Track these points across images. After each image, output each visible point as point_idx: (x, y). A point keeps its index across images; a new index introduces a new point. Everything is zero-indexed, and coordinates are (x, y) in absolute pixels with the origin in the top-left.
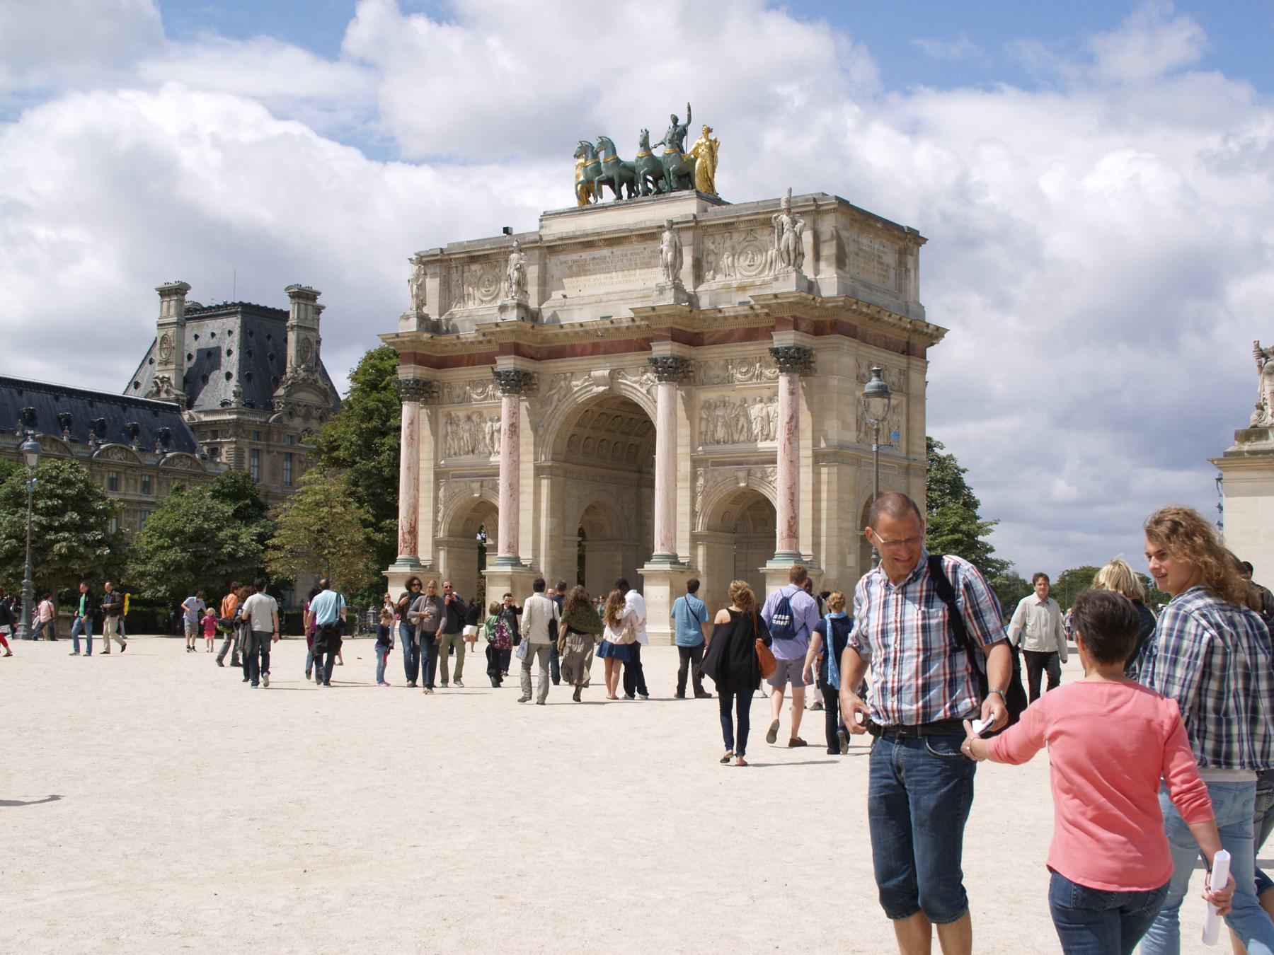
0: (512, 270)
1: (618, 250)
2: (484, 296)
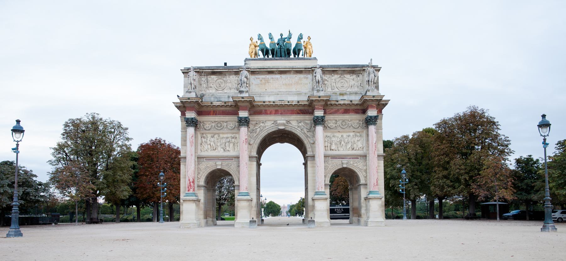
0: (244, 77)
1: (283, 76)
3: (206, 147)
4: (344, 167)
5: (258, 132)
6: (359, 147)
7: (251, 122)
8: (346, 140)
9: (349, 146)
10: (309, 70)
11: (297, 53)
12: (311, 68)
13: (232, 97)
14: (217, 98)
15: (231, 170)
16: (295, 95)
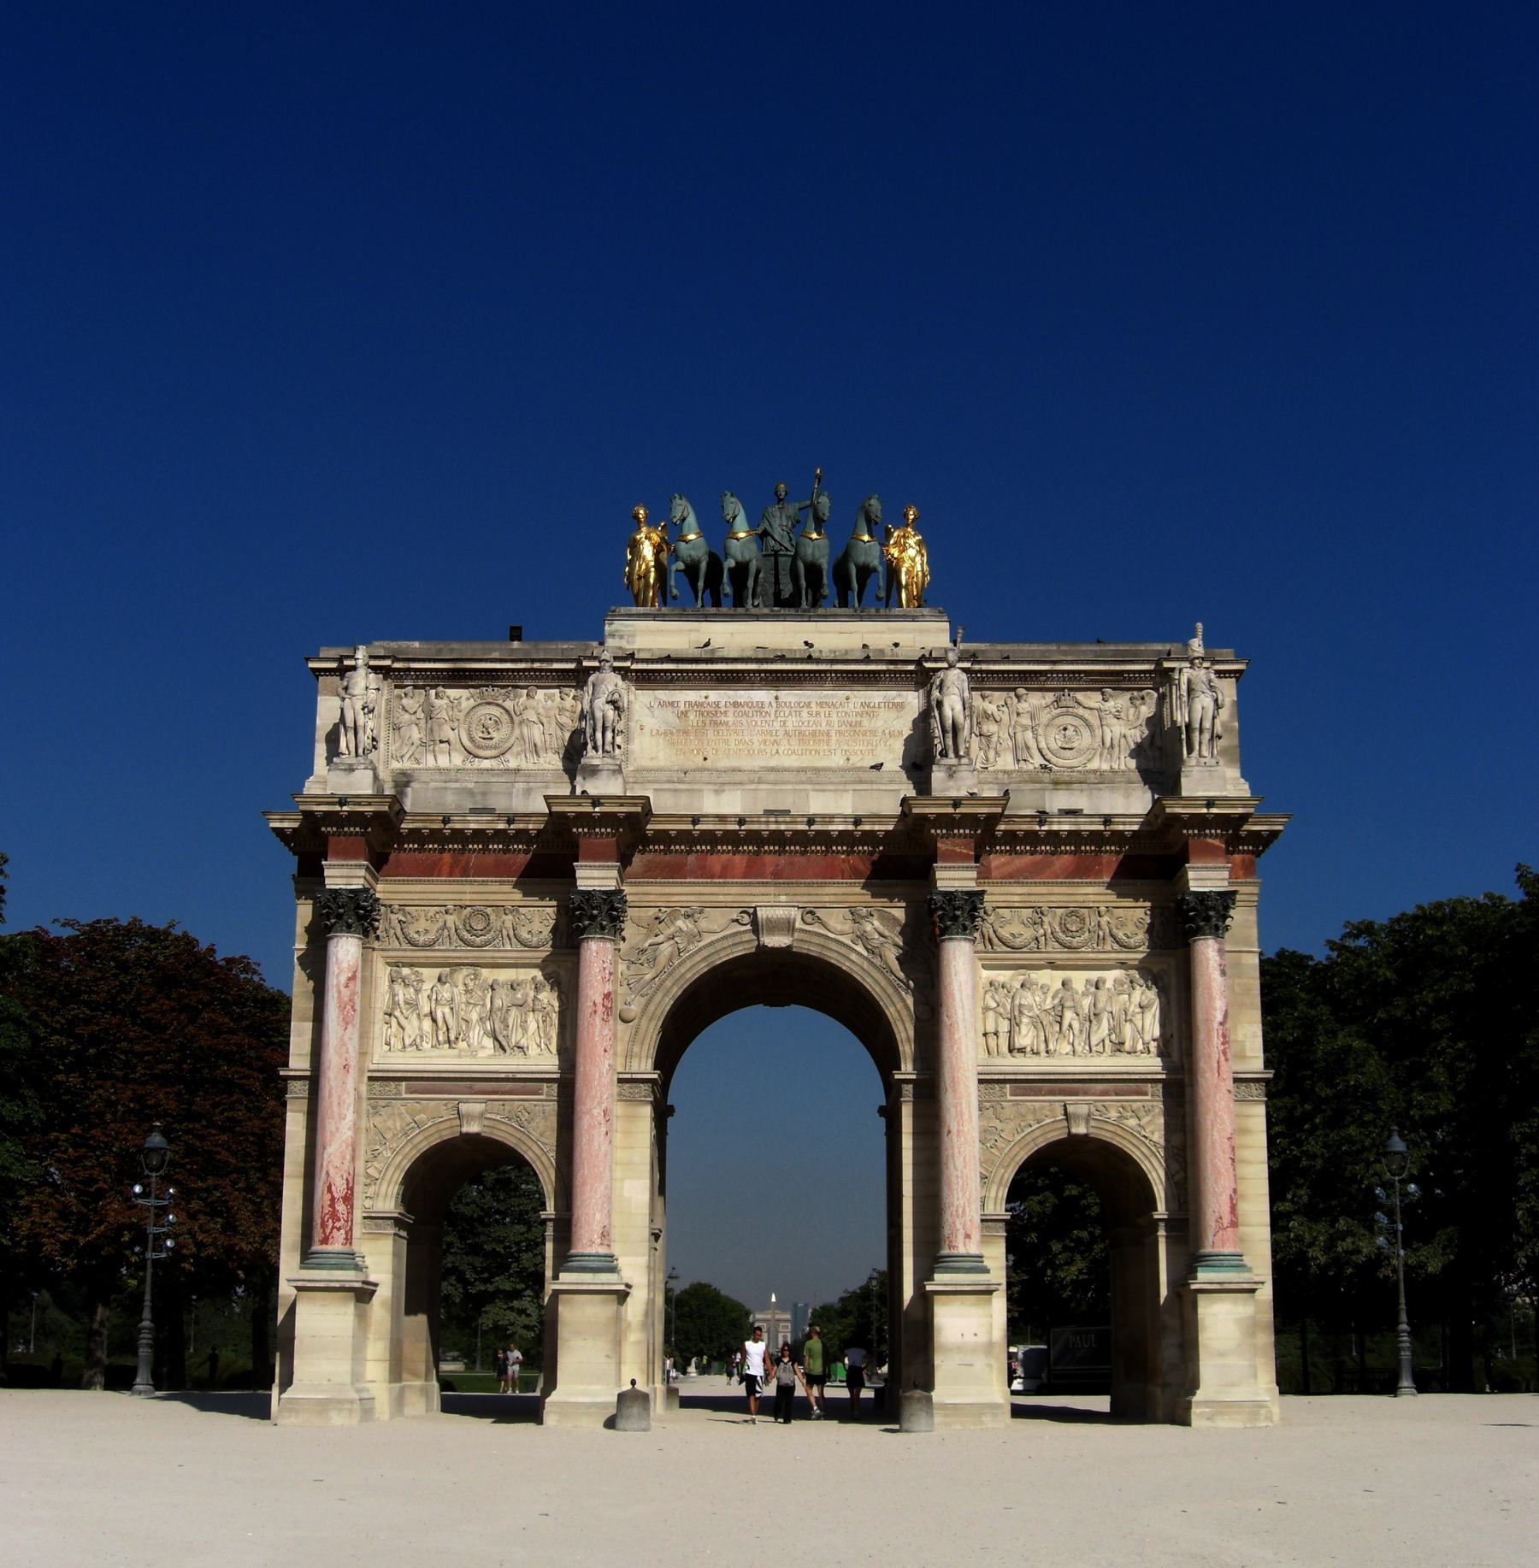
0: (603, 699)
1: (789, 696)
2: (478, 747)
3: (412, 1027)
4: (1077, 1136)
5: (662, 960)
6: (1147, 1038)
7: (630, 911)
8: (1086, 1003)
9: (1102, 1030)
10: (911, 672)
11: (855, 585)
12: (919, 662)
13: (547, 798)
14: (470, 792)
15: (530, 1143)
16: (841, 787)
